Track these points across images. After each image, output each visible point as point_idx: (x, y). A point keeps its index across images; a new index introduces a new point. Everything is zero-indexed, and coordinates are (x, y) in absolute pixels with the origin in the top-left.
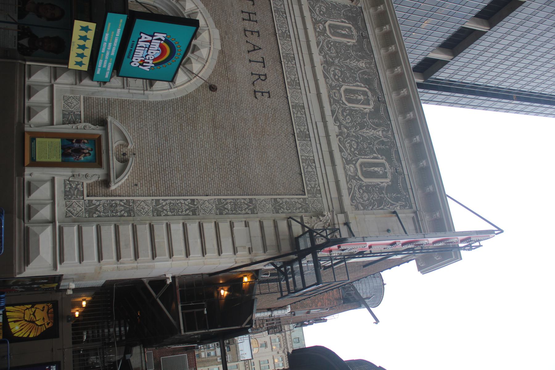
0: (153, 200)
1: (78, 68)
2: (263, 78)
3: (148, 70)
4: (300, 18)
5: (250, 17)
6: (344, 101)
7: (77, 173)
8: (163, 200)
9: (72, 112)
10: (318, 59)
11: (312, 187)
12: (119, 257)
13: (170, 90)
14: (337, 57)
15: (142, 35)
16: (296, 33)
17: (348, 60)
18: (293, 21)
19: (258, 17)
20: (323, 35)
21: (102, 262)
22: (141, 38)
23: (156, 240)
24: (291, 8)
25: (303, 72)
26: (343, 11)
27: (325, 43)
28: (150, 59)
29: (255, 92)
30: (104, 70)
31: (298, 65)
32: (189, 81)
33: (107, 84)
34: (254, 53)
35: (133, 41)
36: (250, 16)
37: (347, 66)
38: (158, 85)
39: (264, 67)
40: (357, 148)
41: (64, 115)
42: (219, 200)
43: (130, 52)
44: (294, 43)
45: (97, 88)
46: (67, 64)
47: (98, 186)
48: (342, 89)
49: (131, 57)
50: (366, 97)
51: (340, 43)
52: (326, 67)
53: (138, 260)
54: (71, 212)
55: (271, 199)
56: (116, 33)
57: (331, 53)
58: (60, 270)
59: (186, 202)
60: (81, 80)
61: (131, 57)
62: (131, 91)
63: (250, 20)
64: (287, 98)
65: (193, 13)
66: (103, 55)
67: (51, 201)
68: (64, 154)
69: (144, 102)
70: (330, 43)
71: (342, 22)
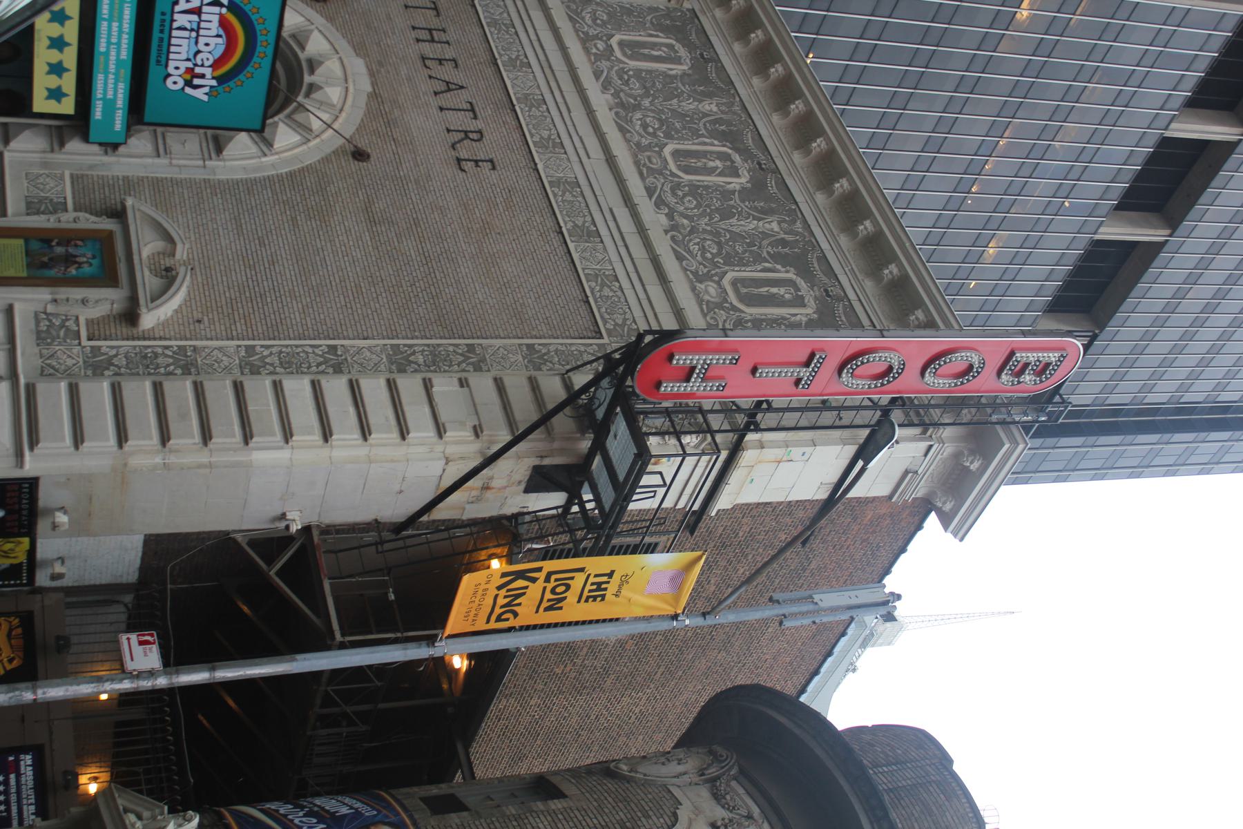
0: (239, 346)
2: (475, 136)
3: (205, 98)
4: (541, 14)
6: (736, 303)
7: (64, 297)
8: (262, 346)
9: (46, 198)
10: (600, 101)
11: (616, 324)
12: (165, 438)
13: (264, 159)
14: (647, 95)
17: (675, 101)
18: (533, 37)
19: (452, 35)
20: (609, 60)
21: (128, 447)
23: (250, 408)
26: (649, 18)
29: (459, 160)
30: (109, 106)
31: (554, 112)
33: (122, 149)
37: (673, 111)
40: (719, 254)
42: (395, 347)
47: (112, 324)
48: (667, 151)
50: (728, 163)
51: (649, 72)
52: (623, 113)
53: (211, 445)
54: (53, 367)
55: (520, 345)
58: (31, 467)
59: (316, 351)
60: (62, 144)
62: (174, 162)
66: (102, 59)
67: (7, 347)
71: (651, 36)
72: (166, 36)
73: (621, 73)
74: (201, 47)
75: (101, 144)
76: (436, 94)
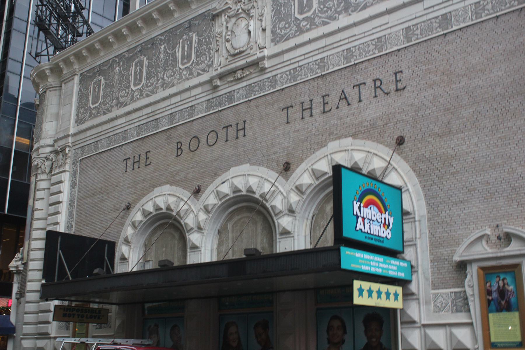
1: (400, 297)
2: (378, 83)
3: (392, 218)
5: (307, 109)
9: (452, 302)
10: (344, 21)
13: (411, 190)
15: (358, 228)
16: (317, 52)
18: (303, 57)
19: (306, 99)
20: (314, 19)
22: (361, 230)
24: (289, 63)
25: (363, 35)
27: (323, 16)
28: (380, 216)
29: (397, 90)
30: (400, 269)
31: (356, 43)
32: (396, 170)
33: (413, 263)
34: (349, 99)
35: (366, 237)
36: (306, 109)
38: (407, 206)
39: (365, 84)
41: (457, 311)
43: (377, 240)
44: (329, 53)
45: (420, 276)
46: (395, 310)
49: (382, 239)
52: (352, 8)
56: (359, 258)
57: (334, 6)
60: (413, 294)
61: (382, 239)
62: (418, 236)
63: (311, 108)
64: (399, 50)
65: (314, 174)
66: (384, 271)
68: (508, 308)
69: (429, 220)
70: (322, 9)
72: (374, 237)
73: (321, 11)
74: (374, 219)
75: (412, 275)
76: (349, 104)
